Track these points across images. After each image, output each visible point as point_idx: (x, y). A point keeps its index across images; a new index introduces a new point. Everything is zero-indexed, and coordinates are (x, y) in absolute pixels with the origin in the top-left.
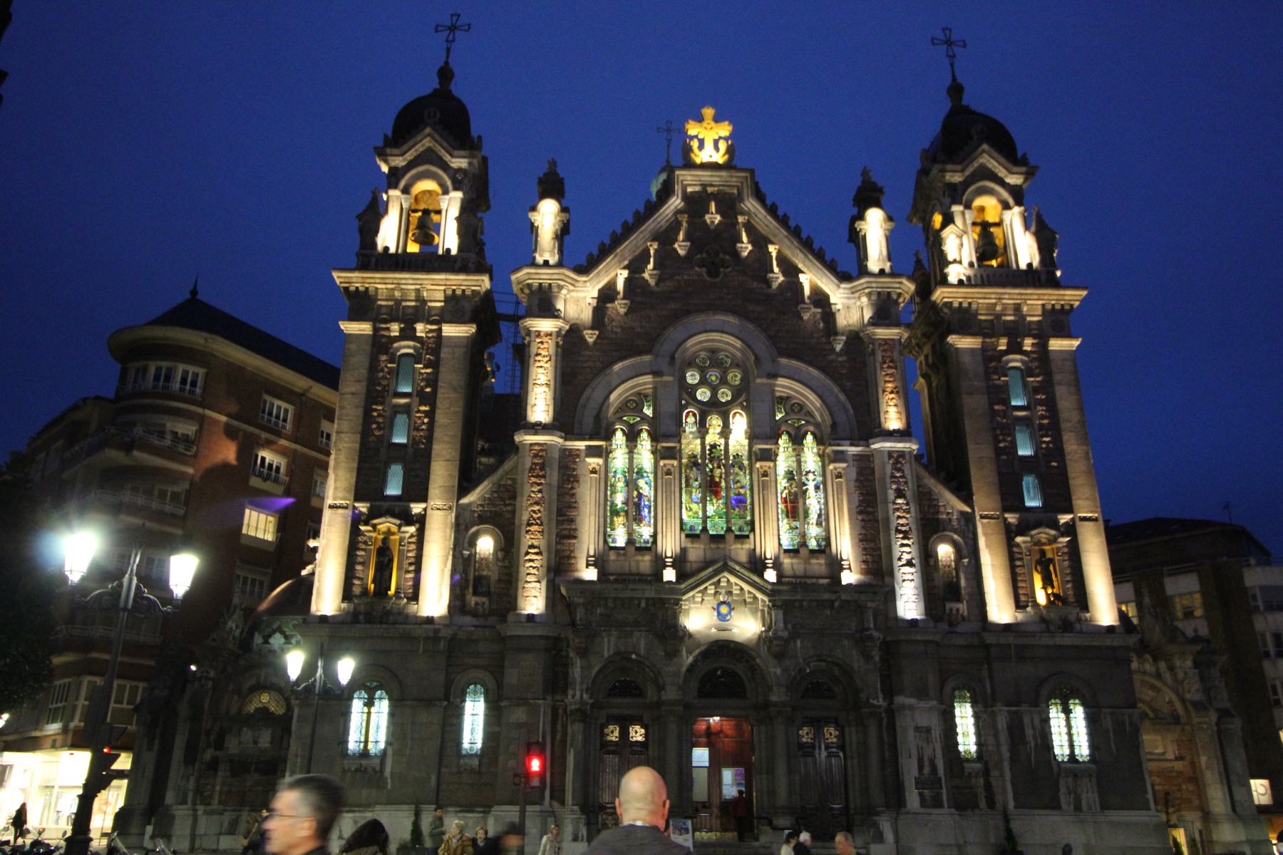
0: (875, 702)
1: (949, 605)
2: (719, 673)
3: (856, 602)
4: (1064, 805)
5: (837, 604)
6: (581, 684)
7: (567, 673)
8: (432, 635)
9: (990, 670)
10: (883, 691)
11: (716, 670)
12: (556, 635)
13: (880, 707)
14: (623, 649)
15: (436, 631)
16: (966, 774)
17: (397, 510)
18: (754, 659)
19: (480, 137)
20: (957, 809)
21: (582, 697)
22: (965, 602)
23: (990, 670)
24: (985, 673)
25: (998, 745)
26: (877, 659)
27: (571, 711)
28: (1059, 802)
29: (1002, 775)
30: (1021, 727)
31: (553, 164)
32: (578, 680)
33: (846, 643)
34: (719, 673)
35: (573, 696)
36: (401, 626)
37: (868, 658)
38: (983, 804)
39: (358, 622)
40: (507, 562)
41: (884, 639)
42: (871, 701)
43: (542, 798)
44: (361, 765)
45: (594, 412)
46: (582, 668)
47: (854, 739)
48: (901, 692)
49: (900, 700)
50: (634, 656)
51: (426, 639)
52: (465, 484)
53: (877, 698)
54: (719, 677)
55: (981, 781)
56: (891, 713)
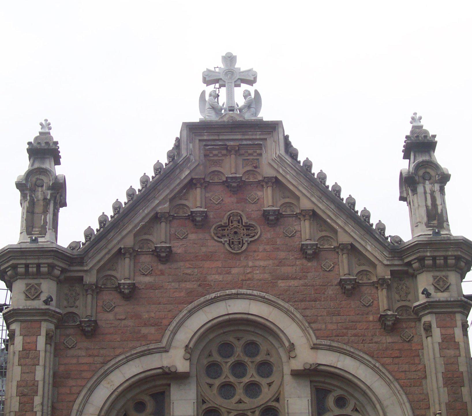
31: (46, 125)
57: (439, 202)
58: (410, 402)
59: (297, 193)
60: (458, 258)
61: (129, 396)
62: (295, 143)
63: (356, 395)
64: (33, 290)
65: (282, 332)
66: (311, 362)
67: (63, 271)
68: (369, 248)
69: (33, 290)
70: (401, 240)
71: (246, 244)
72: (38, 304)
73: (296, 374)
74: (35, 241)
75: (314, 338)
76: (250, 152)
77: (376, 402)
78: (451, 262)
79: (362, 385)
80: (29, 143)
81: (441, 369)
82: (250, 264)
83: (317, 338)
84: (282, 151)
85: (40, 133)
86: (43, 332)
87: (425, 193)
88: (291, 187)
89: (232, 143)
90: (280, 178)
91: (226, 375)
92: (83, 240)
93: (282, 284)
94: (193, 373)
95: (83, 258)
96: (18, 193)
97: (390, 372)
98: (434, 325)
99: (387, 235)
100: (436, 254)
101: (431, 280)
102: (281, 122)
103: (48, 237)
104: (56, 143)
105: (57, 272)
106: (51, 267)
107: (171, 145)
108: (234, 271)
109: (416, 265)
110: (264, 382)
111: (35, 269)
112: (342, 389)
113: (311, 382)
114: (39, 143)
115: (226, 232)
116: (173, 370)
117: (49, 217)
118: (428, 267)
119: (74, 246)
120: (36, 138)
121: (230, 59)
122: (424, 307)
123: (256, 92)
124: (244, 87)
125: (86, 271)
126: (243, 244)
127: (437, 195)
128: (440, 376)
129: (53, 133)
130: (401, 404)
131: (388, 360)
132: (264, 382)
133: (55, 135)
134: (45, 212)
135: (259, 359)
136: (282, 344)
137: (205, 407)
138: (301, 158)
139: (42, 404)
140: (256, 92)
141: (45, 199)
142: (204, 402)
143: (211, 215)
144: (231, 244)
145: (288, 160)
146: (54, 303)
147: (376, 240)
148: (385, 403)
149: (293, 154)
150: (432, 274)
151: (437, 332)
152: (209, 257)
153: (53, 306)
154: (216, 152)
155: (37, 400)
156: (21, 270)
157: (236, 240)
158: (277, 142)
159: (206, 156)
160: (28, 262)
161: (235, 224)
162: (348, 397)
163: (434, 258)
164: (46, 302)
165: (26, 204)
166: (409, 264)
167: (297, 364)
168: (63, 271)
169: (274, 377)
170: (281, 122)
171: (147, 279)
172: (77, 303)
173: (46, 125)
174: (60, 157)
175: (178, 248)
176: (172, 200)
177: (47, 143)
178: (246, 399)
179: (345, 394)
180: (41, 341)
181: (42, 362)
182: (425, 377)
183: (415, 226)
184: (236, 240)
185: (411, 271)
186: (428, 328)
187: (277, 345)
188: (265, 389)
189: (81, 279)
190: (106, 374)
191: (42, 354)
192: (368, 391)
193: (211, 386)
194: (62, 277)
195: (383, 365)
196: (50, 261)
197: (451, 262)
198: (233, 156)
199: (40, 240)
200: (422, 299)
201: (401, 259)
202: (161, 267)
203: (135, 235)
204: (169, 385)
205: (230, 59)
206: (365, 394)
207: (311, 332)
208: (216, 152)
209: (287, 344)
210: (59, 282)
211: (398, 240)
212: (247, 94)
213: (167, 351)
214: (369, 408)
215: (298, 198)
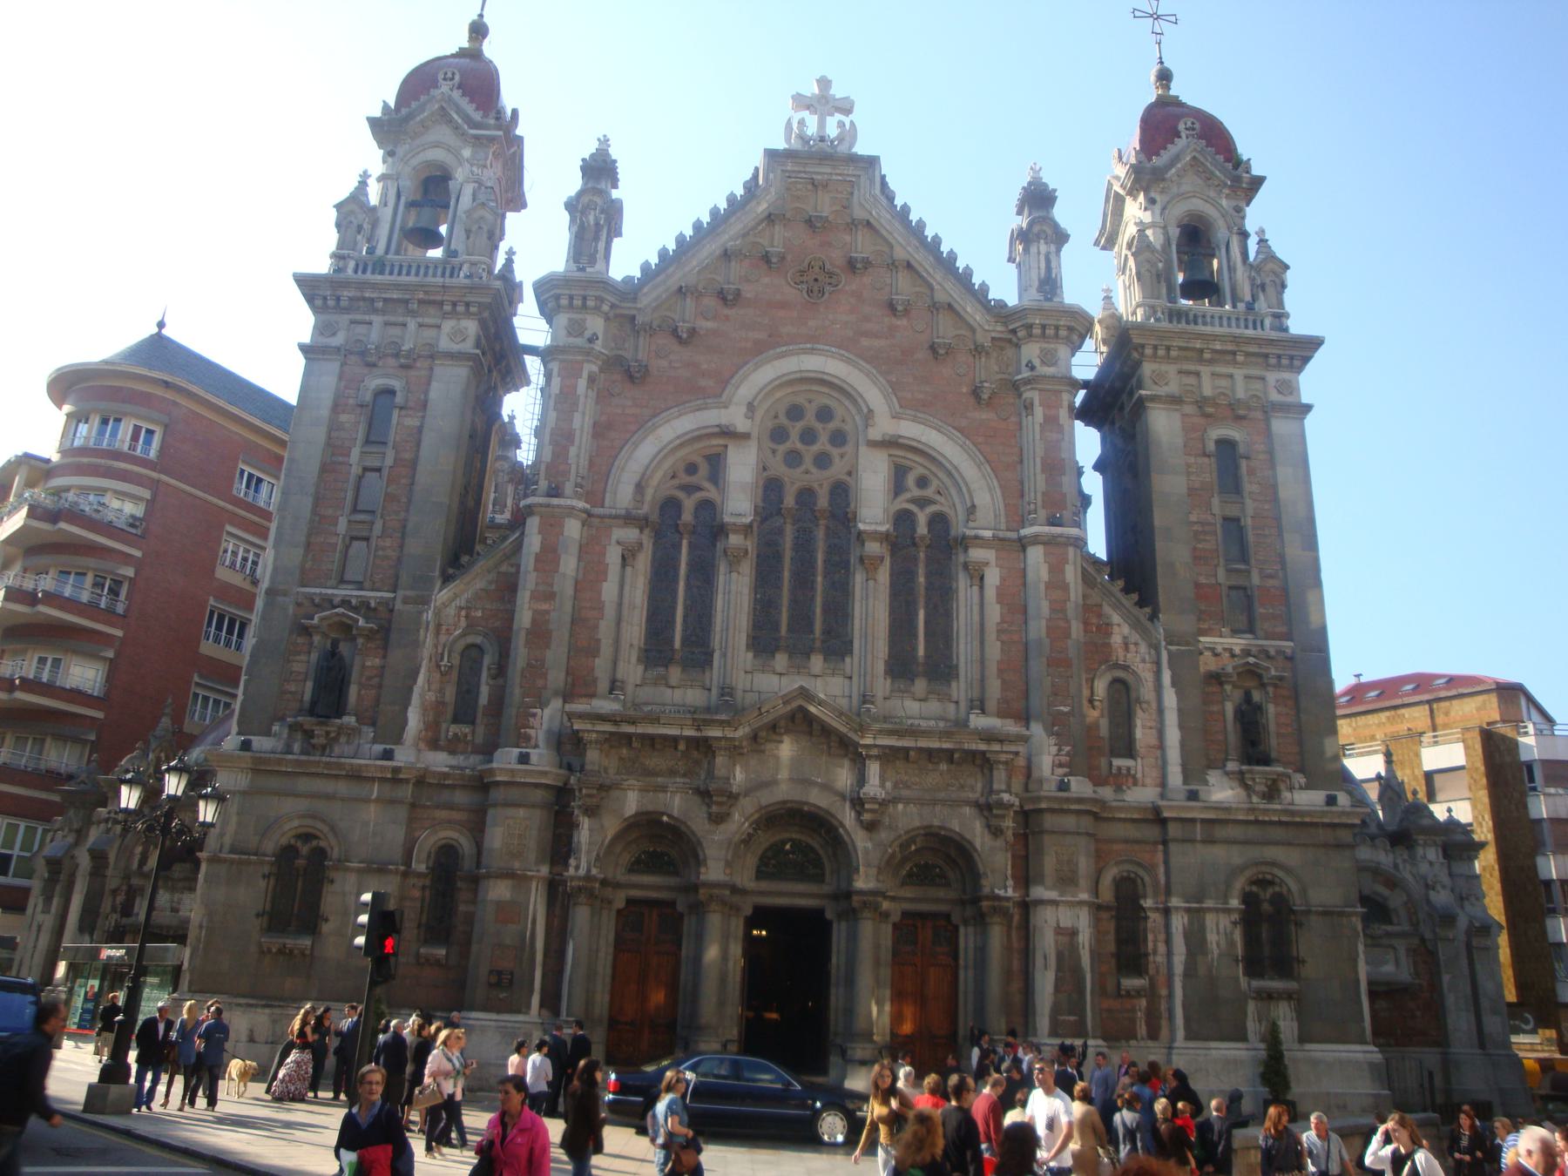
0: (1001, 893)
1: (1117, 762)
2: (788, 847)
3: (983, 753)
4: (1251, 1035)
5: (956, 756)
6: (588, 852)
7: (571, 837)
8: (389, 776)
9: (1166, 853)
10: (1014, 877)
11: (784, 843)
12: (560, 784)
13: (1008, 899)
14: (650, 808)
15: (396, 770)
16: (1123, 993)
17: (354, 602)
18: (837, 830)
19: (515, 112)
20: (1105, 1039)
21: (589, 870)
22: (1139, 760)
23: (1166, 853)
24: (1160, 856)
25: (1169, 954)
26: (1010, 833)
27: (572, 888)
28: (1244, 1029)
29: (1171, 996)
30: (1202, 929)
31: (604, 142)
32: (584, 848)
33: (967, 810)
34: (788, 847)
35: (577, 868)
36: (348, 761)
37: (996, 832)
38: (1142, 1030)
39: (290, 752)
40: (501, 681)
41: (1021, 806)
42: (997, 891)
43: (528, 1006)
44: (284, 945)
45: (636, 478)
46: (590, 830)
47: (971, 945)
48: (1040, 880)
49: (1038, 892)
50: (665, 818)
51: (382, 780)
52: (451, 571)
53: (1005, 888)
54: (788, 853)
55: (1143, 1002)
56: (1026, 907)
57: (1053, 265)
58: (1001, 487)
59: (891, 240)
60: (1070, 329)
61: (681, 454)
62: (893, 184)
63: (940, 474)
65: (861, 396)
66: (891, 433)
67: (613, 306)
68: (969, 309)
70: (1006, 305)
72: (579, 341)
73: (874, 444)
74: (582, 270)
75: (897, 406)
77: (962, 485)
78: (1063, 333)
79: (947, 465)
80: (583, 160)
81: (1040, 452)
82: (831, 317)
83: (901, 407)
84: (877, 191)
86: (585, 375)
87: (1039, 253)
88: (885, 233)
89: (819, 177)
90: (872, 220)
91: (794, 442)
92: (639, 275)
93: (865, 342)
94: (755, 434)
95: (636, 294)
96: (566, 217)
97: (981, 453)
98: (1036, 402)
99: (990, 297)
100: (1046, 322)
102: (878, 158)
103: (599, 266)
104: (615, 161)
105: (606, 308)
107: (748, 175)
108: (811, 323)
109: (1021, 334)
110: (835, 452)
112: (925, 467)
113: (890, 455)
115: (805, 279)
116: (732, 429)
117: (601, 245)
119: (628, 280)
120: (592, 155)
121: (824, 83)
122: (1027, 382)
123: (852, 122)
124: (838, 117)
125: (639, 309)
127: (1053, 257)
128: (1038, 460)
129: (611, 151)
130: (990, 490)
131: (980, 439)
132: (835, 452)
133: (614, 153)
134: (596, 238)
135: (832, 426)
136: (859, 410)
137: (765, 474)
138: (899, 202)
139: (578, 456)
140: (852, 122)
141: (597, 224)
142: (765, 469)
143: (789, 257)
144: (810, 292)
145: (884, 201)
146: (599, 342)
147: (980, 302)
148: (973, 487)
149: (890, 198)
150: (1038, 345)
151: (1039, 412)
152: (783, 305)
153: (598, 346)
154: (799, 186)
155: (573, 451)
156: (564, 302)
157: (816, 289)
158: (872, 182)
159: (788, 189)
160: (574, 292)
161: (817, 269)
162: (932, 477)
163: (1044, 327)
164: (590, 340)
165: (575, 228)
166: (1014, 332)
167: (875, 434)
168: (613, 306)
169: (849, 448)
170: (878, 158)
171: (710, 325)
172: (626, 345)
173: (604, 142)
174: (618, 180)
175: (748, 291)
176: (744, 236)
178: (814, 470)
179: (927, 472)
180: (582, 384)
181: (581, 408)
182: (1021, 462)
183: (1023, 289)
184: (816, 289)
185: (1015, 340)
186: (1029, 407)
187: (854, 411)
188: (837, 460)
190: (655, 427)
191: (582, 399)
192: (953, 471)
193: (774, 452)
194: (611, 315)
195: (975, 444)
196: (598, 293)
199: (588, 270)
200: (1026, 374)
201: (1005, 324)
202: (726, 311)
204: (726, 446)
205: (824, 83)
206: (950, 474)
207: (895, 400)
208: (799, 186)
209: (865, 410)
210: (607, 319)
211: (1001, 304)
212: (841, 124)
213: (726, 407)
214: (953, 492)
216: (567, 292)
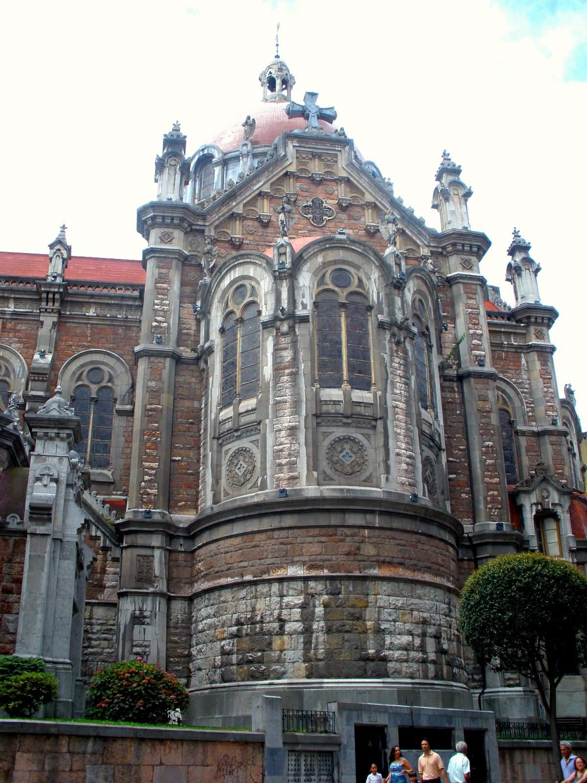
64: (166, 237)
69: (166, 237)
71: (325, 222)
76: (329, 158)
80: (165, 135)
85: (173, 130)
101: (459, 261)
106: (182, 220)
109: (450, 249)
111: (169, 221)
114: (172, 136)
118: (458, 251)
126: (323, 221)
133: (183, 132)
177: (178, 136)
189: (203, 231)
197: (475, 249)
198: (316, 160)
201: (439, 243)
203: (245, 205)
215: (363, 194)
216: (162, 214)
